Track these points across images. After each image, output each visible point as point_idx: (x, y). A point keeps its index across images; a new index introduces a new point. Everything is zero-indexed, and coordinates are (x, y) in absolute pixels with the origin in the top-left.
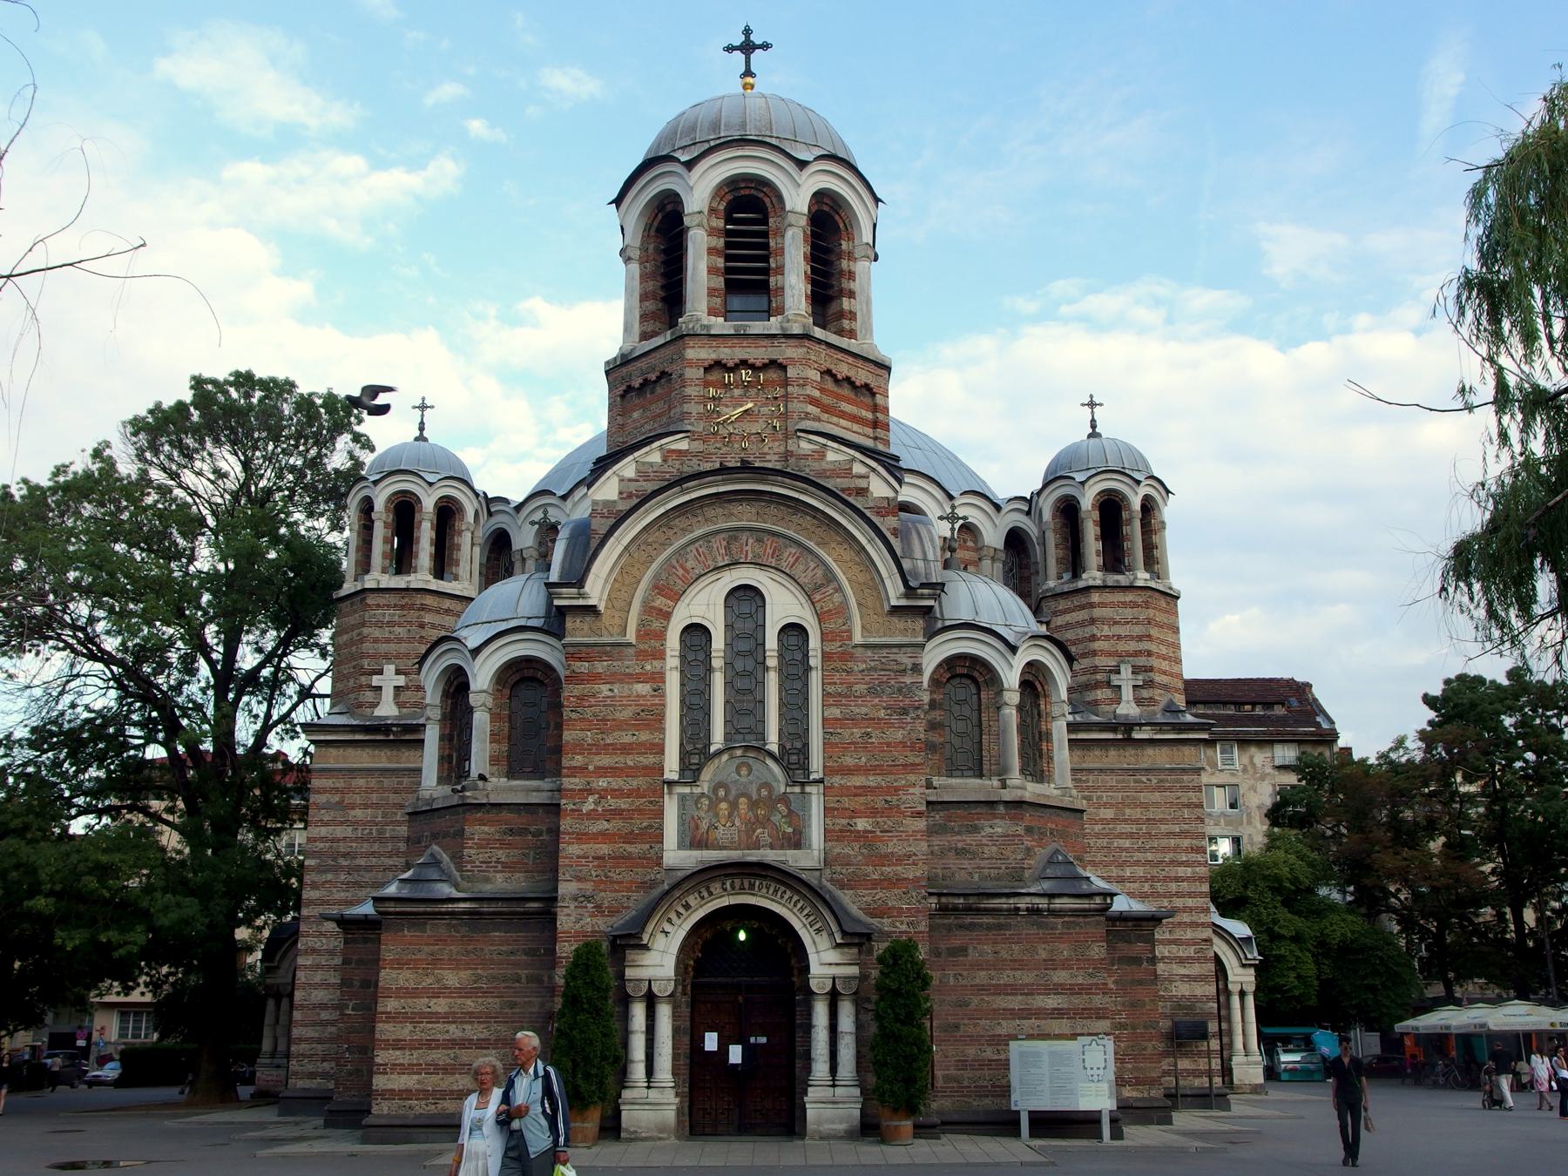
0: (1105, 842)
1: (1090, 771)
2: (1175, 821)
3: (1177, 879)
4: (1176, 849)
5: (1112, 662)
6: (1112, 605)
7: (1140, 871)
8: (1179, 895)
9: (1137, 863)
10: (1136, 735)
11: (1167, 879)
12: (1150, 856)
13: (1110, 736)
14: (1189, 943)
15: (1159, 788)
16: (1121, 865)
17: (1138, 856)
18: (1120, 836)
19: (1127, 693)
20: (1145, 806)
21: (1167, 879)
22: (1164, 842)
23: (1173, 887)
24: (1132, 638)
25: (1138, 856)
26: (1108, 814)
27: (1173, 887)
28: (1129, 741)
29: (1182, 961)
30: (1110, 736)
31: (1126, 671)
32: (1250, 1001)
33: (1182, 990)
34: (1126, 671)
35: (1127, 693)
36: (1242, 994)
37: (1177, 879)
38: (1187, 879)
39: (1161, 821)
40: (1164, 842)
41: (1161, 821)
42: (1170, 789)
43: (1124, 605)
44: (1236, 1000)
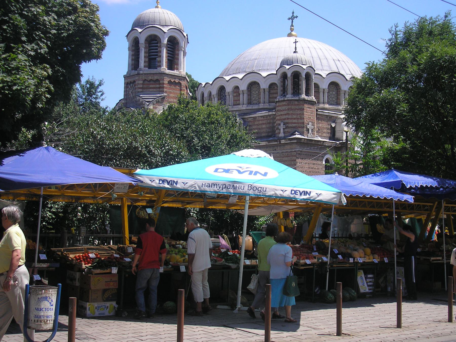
10: (282, 142)
13: (276, 143)
15: (287, 156)
28: (281, 145)
30: (276, 143)
35: (282, 131)
42: (289, 156)
43: (283, 105)
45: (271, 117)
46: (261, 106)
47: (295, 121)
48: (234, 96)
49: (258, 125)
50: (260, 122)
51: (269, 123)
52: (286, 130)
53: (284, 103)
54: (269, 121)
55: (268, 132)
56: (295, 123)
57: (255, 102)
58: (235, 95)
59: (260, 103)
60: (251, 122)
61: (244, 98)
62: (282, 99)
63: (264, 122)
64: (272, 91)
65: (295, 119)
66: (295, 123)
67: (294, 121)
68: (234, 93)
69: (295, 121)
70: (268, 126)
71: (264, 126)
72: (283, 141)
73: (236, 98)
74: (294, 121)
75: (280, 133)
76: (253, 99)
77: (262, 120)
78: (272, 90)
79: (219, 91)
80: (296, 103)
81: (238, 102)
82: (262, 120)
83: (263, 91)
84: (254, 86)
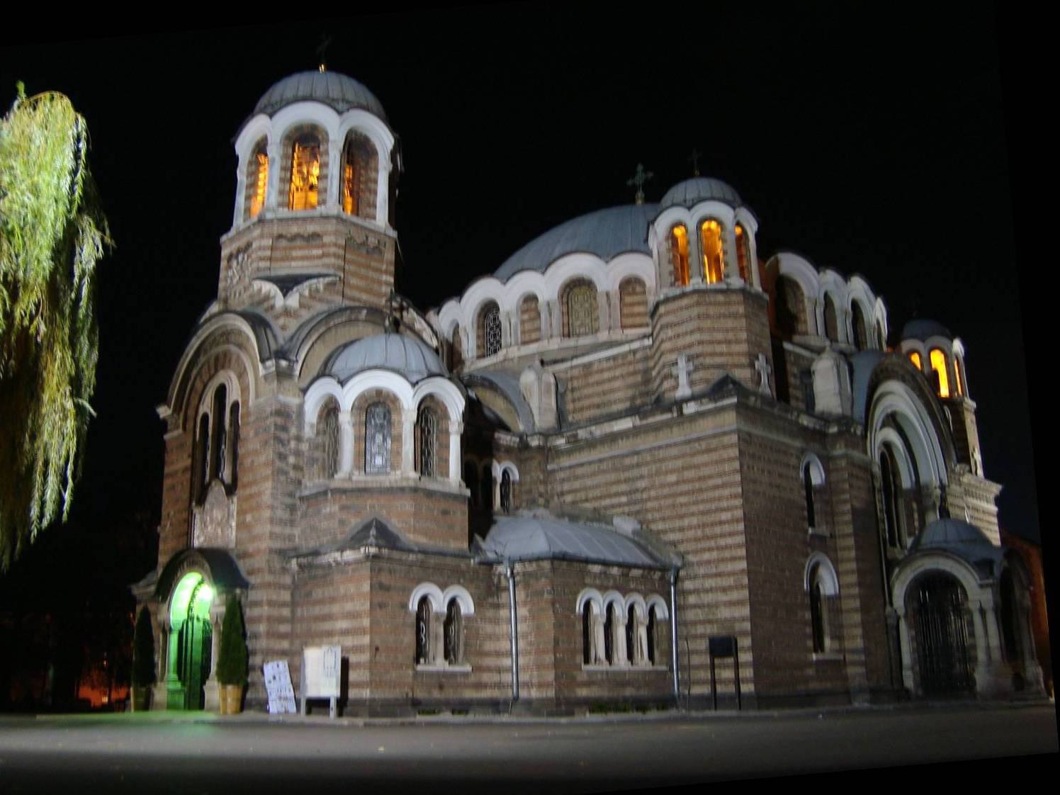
0: (670, 501)
1: (660, 448)
2: (720, 475)
3: (721, 523)
4: (720, 499)
5: (672, 357)
6: (674, 312)
7: (694, 521)
8: (722, 535)
9: (693, 514)
11: (713, 524)
12: (701, 507)
14: (730, 574)
16: (682, 517)
17: (694, 509)
18: (681, 494)
19: (683, 379)
20: (697, 467)
21: (713, 524)
22: (711, 494)
23: (718, 530)
24: (686, 333)
25: (694, 509)
26: (672, 478)
27: (718, 530)
29: (724, 590)
31: (682, 363)
32: (991, 618)
33: (725, 613)
34: (682, 363)
35: (683, 379)
36: (983, 612)
37: (721, 523)
38: (727, 522)
39: (710, 477)
40: (711, 494)
41: (710, 477)
42: (715, 450)
44: (977, 619)
45: (639, 356)
46: (603, 336)
47: (724, 348)
48: (523, 322)
49: (598, 383)
50: (606, 375)
51: (634, 373)
52: (696, 376)
53: (685, 302)
54: (631, 369)
55: (633, 398)
56: (721, 354)
57: (582, 330)
58: (526, 317)
59: (597, 331)
60: (577, 378)
61: (551, 321)
62: (678, 291)
63: (618, 372)
64: (628, 299)
65: (720, 342)
66: (721, 354)
67: (719, 348)
68: (524, 312)
69: (724, 348)
70: (631, 380)
71: (617, 384)
72: (690, 408)
73: (528, 326)
74: (719, 348)
75: (676, 387)
76: (578, 323)
77: (609, 369)
78: (629, 294)
79: (479, 315)
80: (721, 298)
81: (534, 336)
82: (609, 369)
83: (605, 297)
84: (576, 290)
